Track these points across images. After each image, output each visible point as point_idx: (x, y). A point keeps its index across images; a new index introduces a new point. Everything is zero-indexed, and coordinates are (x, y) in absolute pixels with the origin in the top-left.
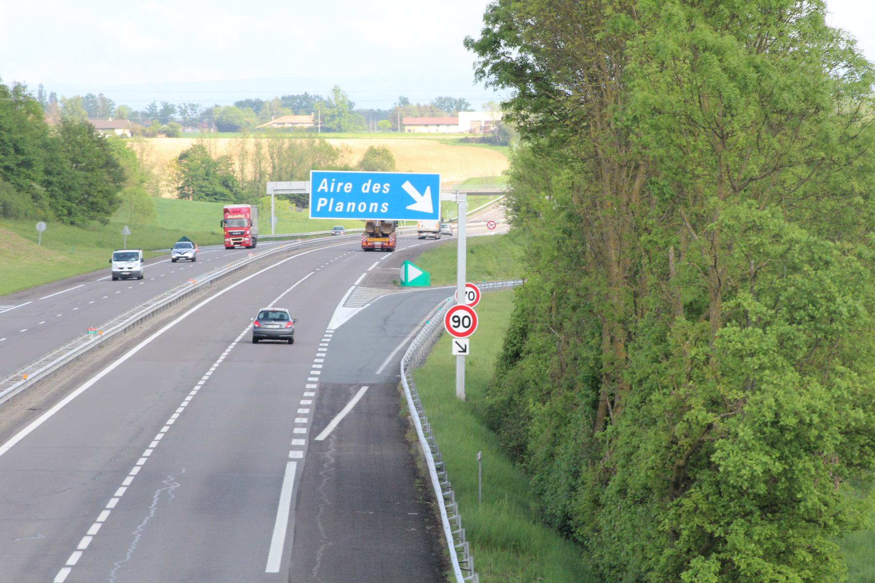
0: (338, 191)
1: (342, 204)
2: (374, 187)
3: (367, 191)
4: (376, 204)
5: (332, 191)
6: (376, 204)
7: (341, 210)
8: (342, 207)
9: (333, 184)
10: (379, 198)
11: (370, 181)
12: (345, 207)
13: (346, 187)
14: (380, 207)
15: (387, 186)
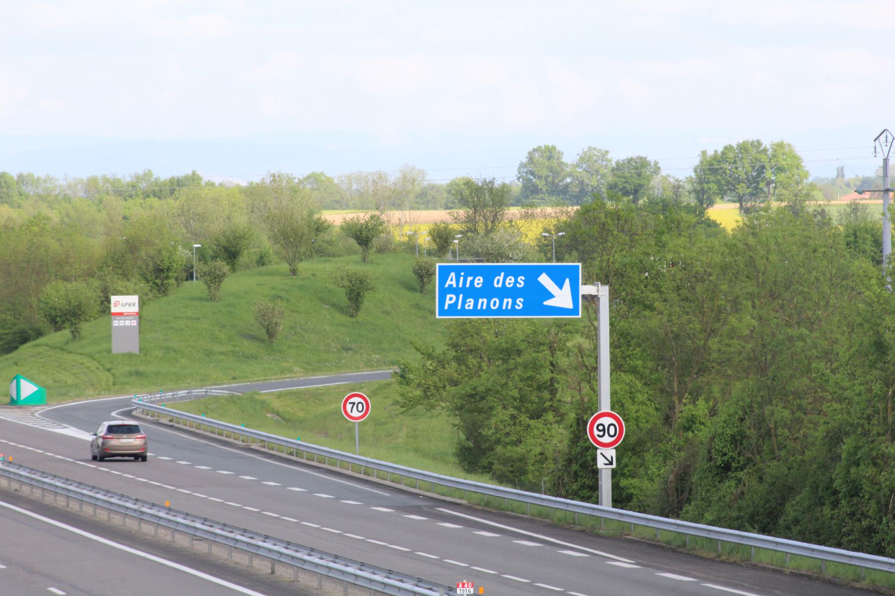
1: (472, 301)
2: (508, 281)
3: (500, 285)
7: (471, 308)
8: (472, 304)
9: (462, 278)
10: (513, 293)
13: (476, 281)
14: (514, 303)
15: (521, 279)
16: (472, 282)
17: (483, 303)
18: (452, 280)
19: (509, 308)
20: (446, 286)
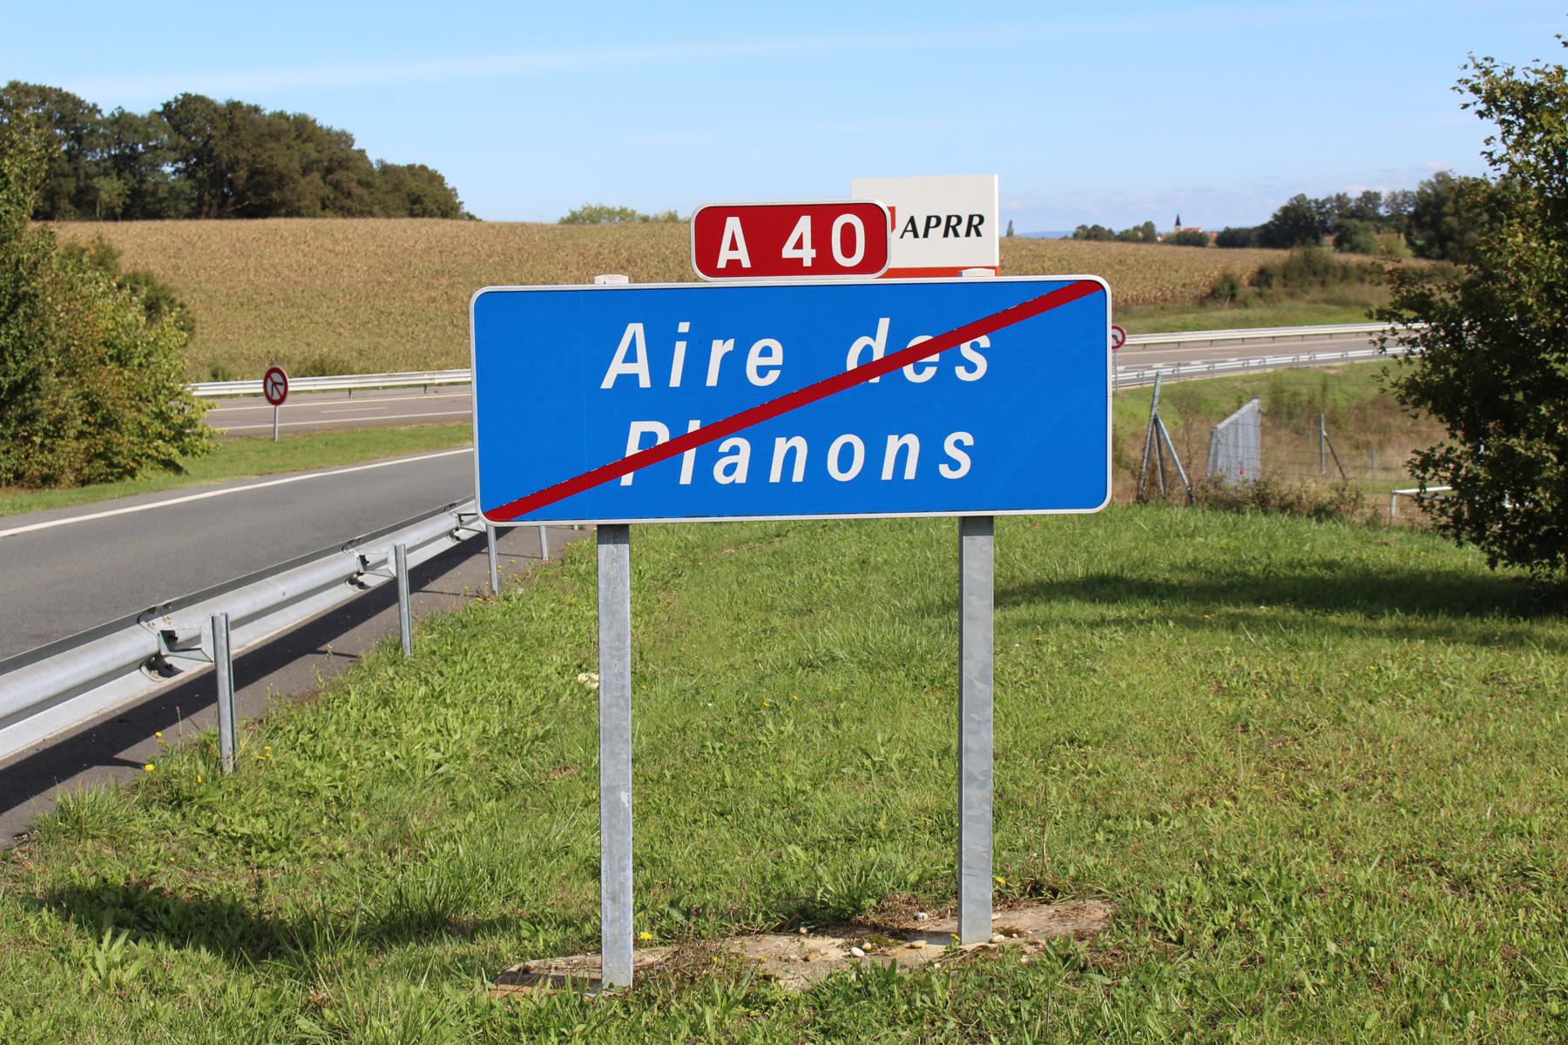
0: (712, 380)
1: (744, 445)
4: (912, 440)
5: (675, 380)
6: (912, 440)
7: (740, 476)
8: (743, 460)
9: (680, 348)
11: (884, 324)
12: (760, 461)
13: (754, 360)
14: (932, 454)
16: (735, 363)
17: (791, 453)
18: (631, 357)
19: (910, 473)
20: (608, 383)
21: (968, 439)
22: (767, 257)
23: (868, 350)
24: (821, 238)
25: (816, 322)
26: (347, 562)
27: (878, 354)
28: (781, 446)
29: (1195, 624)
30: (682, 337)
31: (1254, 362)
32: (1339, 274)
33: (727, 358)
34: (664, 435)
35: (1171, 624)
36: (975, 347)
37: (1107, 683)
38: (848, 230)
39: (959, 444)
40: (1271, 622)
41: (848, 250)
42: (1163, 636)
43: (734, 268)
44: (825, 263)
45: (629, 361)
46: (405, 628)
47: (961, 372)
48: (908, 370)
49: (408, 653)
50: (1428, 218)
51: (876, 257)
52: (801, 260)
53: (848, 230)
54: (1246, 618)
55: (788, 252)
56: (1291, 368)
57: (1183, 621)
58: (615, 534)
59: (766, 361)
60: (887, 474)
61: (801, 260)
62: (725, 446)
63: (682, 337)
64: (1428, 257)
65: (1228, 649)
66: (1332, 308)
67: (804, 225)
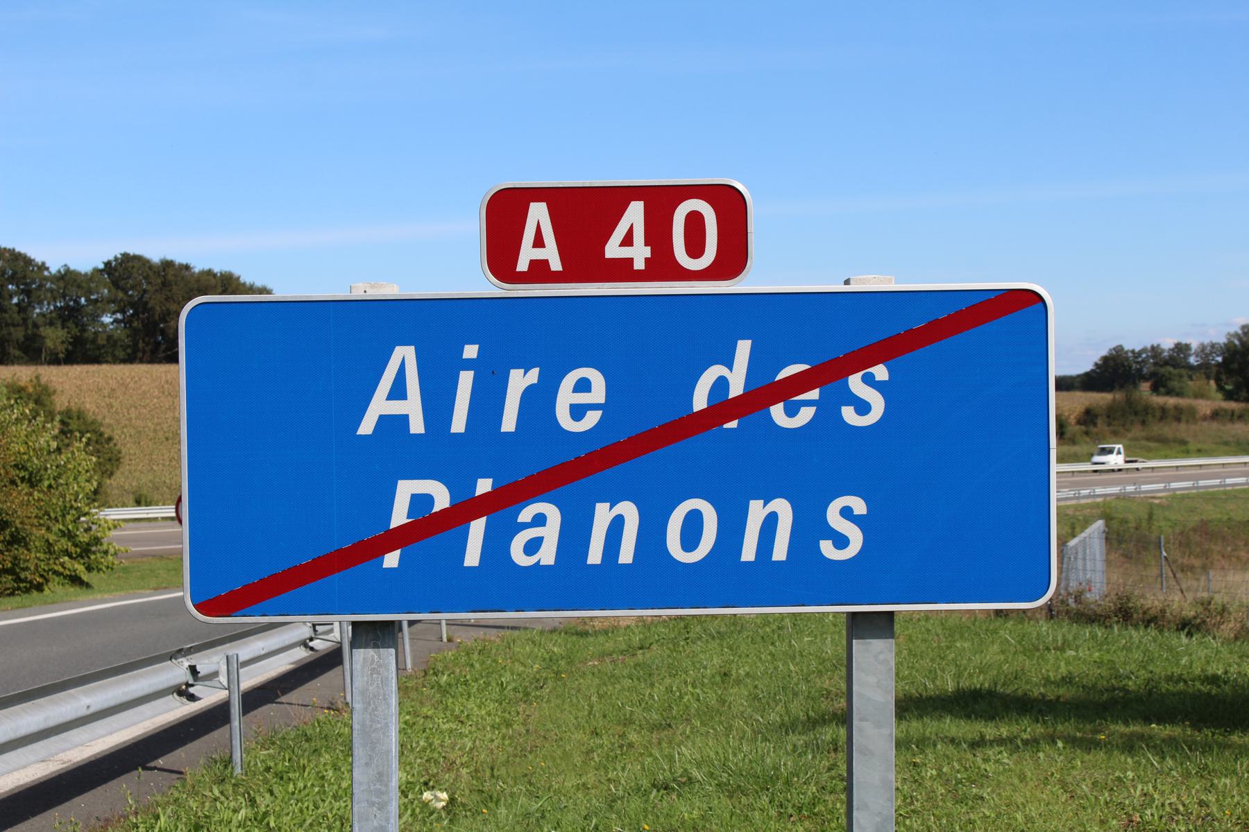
0: (509, 423)
1: (553, 513)
4: (783, 508)
5: (459, 424)
7: (547, 555)
8: (551, 533)
9: (466, 380)
11: (744, 348)
12: (574, 535)
13: (566, 397)
14: (810, 527)
17: (617, 525)
18: (398, 391)
19: (780, 552)
20: (367, 427)
21: (859, 506)
22: (584, 258)
23: (722, 383)
24: (658, 233)
25: (649, 347)
26: (177, 672)
27: (736, 388)
28: (603, 515)
29: (1089, 745)
30: (469, 364)
31: (1085, 492)
32: (1158, 414)
33: (528, 393)
34: (442, 499)
35: (1060, 744)
36: (869, 380)
37: (999, 815)
38: (695, 221)
39: (846, 513)
40: (1171, 741)
41: (695, 249)
42: (1053, 758)
43: (539, 271)
44: (661, 266)
45: (395, 397)
46: (236, 743)
47: (849, 415)
48: (777, 412)
49: (238, 770)
50: (1235, 366)
51: (733, 259)
52: (631, 261)
53: (695, 221)
54: (1141, 737)
55: (613, 250)
56: (1118, 497)
57: (1072, 741)
58: (374, 634)
59: (582, 398)
60: (749, 553)
61: (631, 261)
62: (526, 515)
63: (469, 364)
64: (1237, 400)
65: (1130, 774)
66: (1152, 445)
67: (635, 214)
